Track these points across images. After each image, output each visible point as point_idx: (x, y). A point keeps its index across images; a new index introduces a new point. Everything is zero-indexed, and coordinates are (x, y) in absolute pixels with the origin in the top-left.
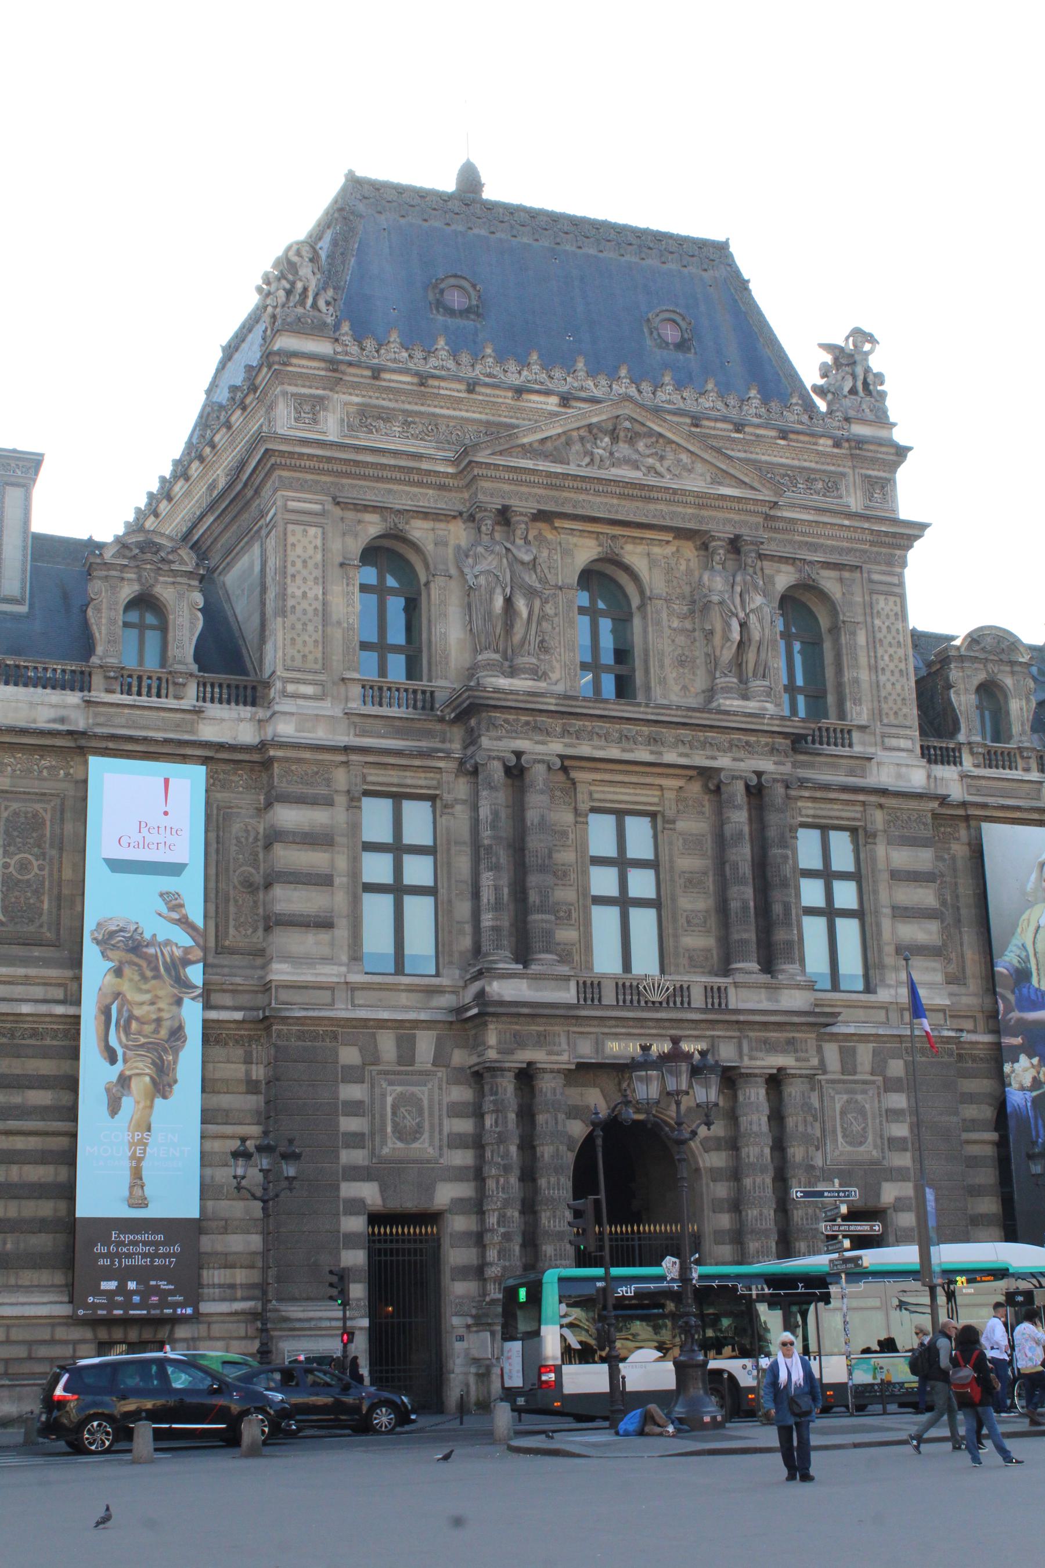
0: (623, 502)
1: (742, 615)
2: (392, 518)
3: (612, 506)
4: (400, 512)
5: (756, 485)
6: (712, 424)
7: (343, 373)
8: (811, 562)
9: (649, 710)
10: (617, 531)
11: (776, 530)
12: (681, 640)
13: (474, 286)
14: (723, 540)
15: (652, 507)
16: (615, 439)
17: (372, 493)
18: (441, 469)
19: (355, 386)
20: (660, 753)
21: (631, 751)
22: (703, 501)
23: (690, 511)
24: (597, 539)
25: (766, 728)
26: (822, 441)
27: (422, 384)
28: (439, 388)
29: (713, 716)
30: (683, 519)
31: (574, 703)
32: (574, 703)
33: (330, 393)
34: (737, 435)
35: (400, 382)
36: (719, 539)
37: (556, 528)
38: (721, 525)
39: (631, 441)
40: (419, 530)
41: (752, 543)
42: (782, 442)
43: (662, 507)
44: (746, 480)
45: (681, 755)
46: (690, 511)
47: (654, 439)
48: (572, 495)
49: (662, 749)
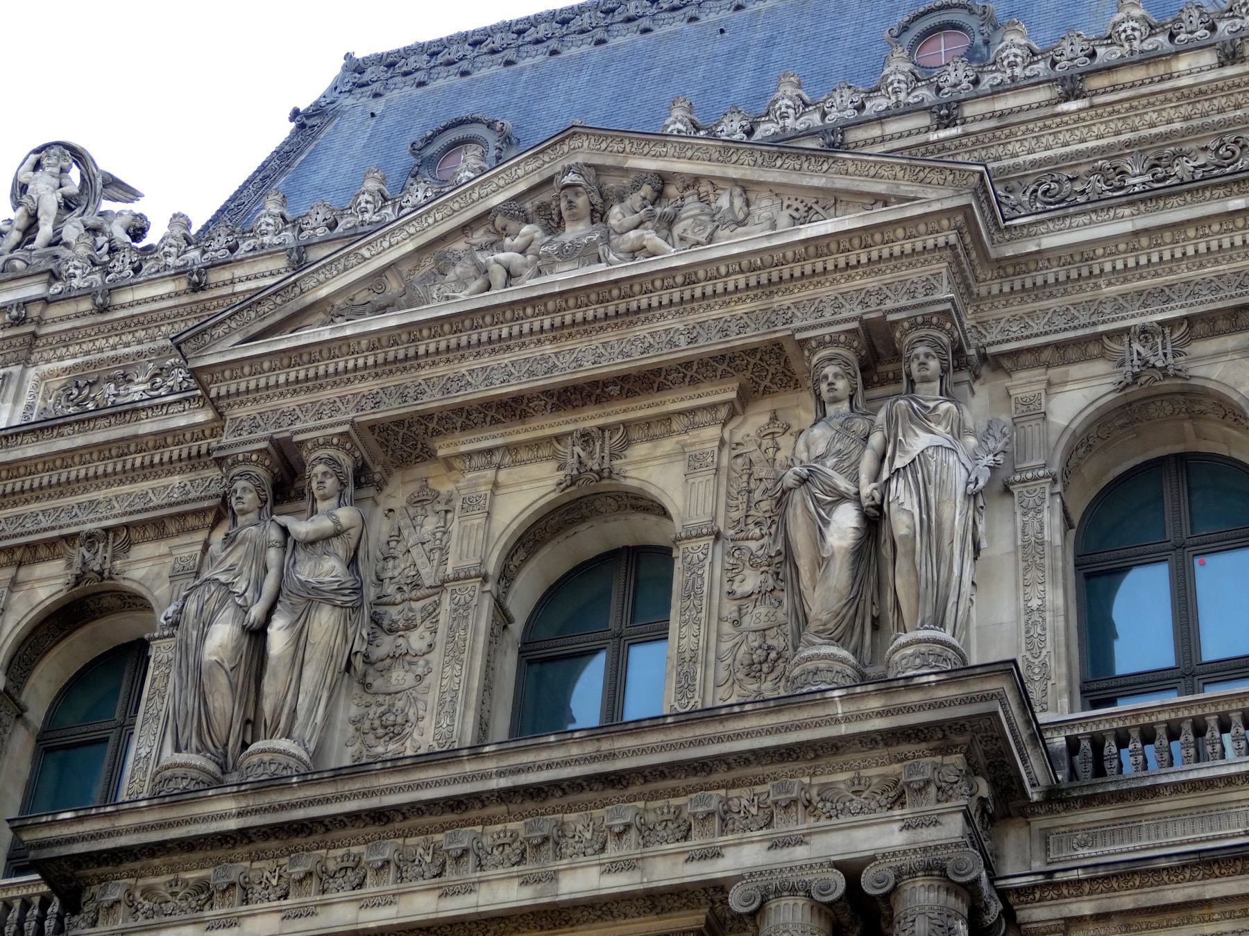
0: (568, 345)
1: (867, 489)
2: (79, 553)
3: (546, 359)
4: (90, 539)
5: (906, 188)
6: (876, 132)
7: (40, 322)
8: (1145, 333)
9: (490, 765)
10: (591, 418)
11: (1038, 291)
12: (758, 615)
13: (490, 125)
14: (834, 342)
15: (641, 330)
16: (554, 225)
17: (40, 517)
18: (182, 422)
19: (67, 339)
20: (553, 877)
21: (469, 889)
22: (768, 273)
23: (740, 309)
24: (554, 456)
25: (843, 729)
26: (1182, 64)
27: (196, 287)
28: (232, 282)
29: (675, 735)
30: (724, 332)
31: (285, 797)
32: (285, 797)
33: (16, 370)
34: (943, 134)
35: (154, 299)
36: (822, 344)
37: (448, 462)
38: (824, 311)
39: (598, 214)
40: (145, 568)
41: (915, 326)
42: (1072, 106)
43: (672, 322)
44: (880, 188)
45: (614, 867)
46: (740, 309)
47: (646, 190)
48: (442, 370)
49: (553, 865)
